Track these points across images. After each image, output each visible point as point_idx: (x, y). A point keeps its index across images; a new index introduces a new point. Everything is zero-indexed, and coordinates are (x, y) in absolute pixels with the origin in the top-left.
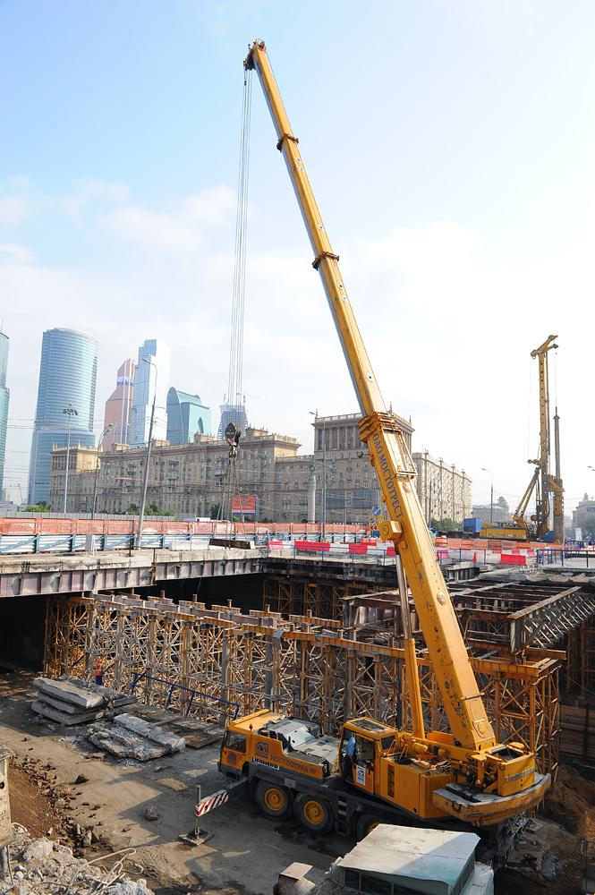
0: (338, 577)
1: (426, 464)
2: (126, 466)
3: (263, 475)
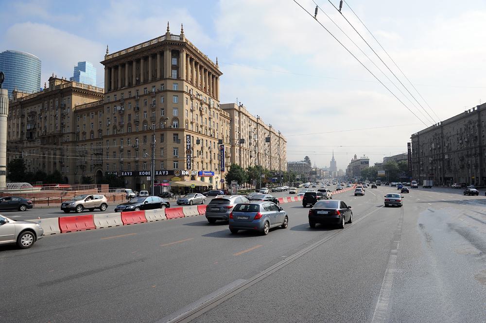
3: (63, 126)
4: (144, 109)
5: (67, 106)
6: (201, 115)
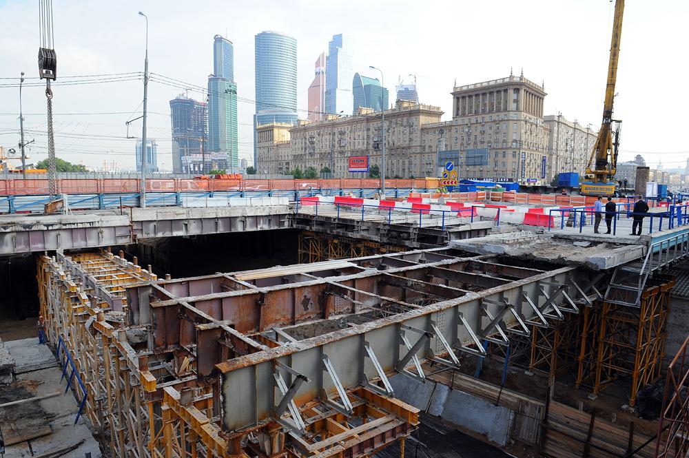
0: (350, 234)
1: (558, 125)
2: (308, 137)
4: (488, 132)
5: (415, 124)
6: (531, 134)
